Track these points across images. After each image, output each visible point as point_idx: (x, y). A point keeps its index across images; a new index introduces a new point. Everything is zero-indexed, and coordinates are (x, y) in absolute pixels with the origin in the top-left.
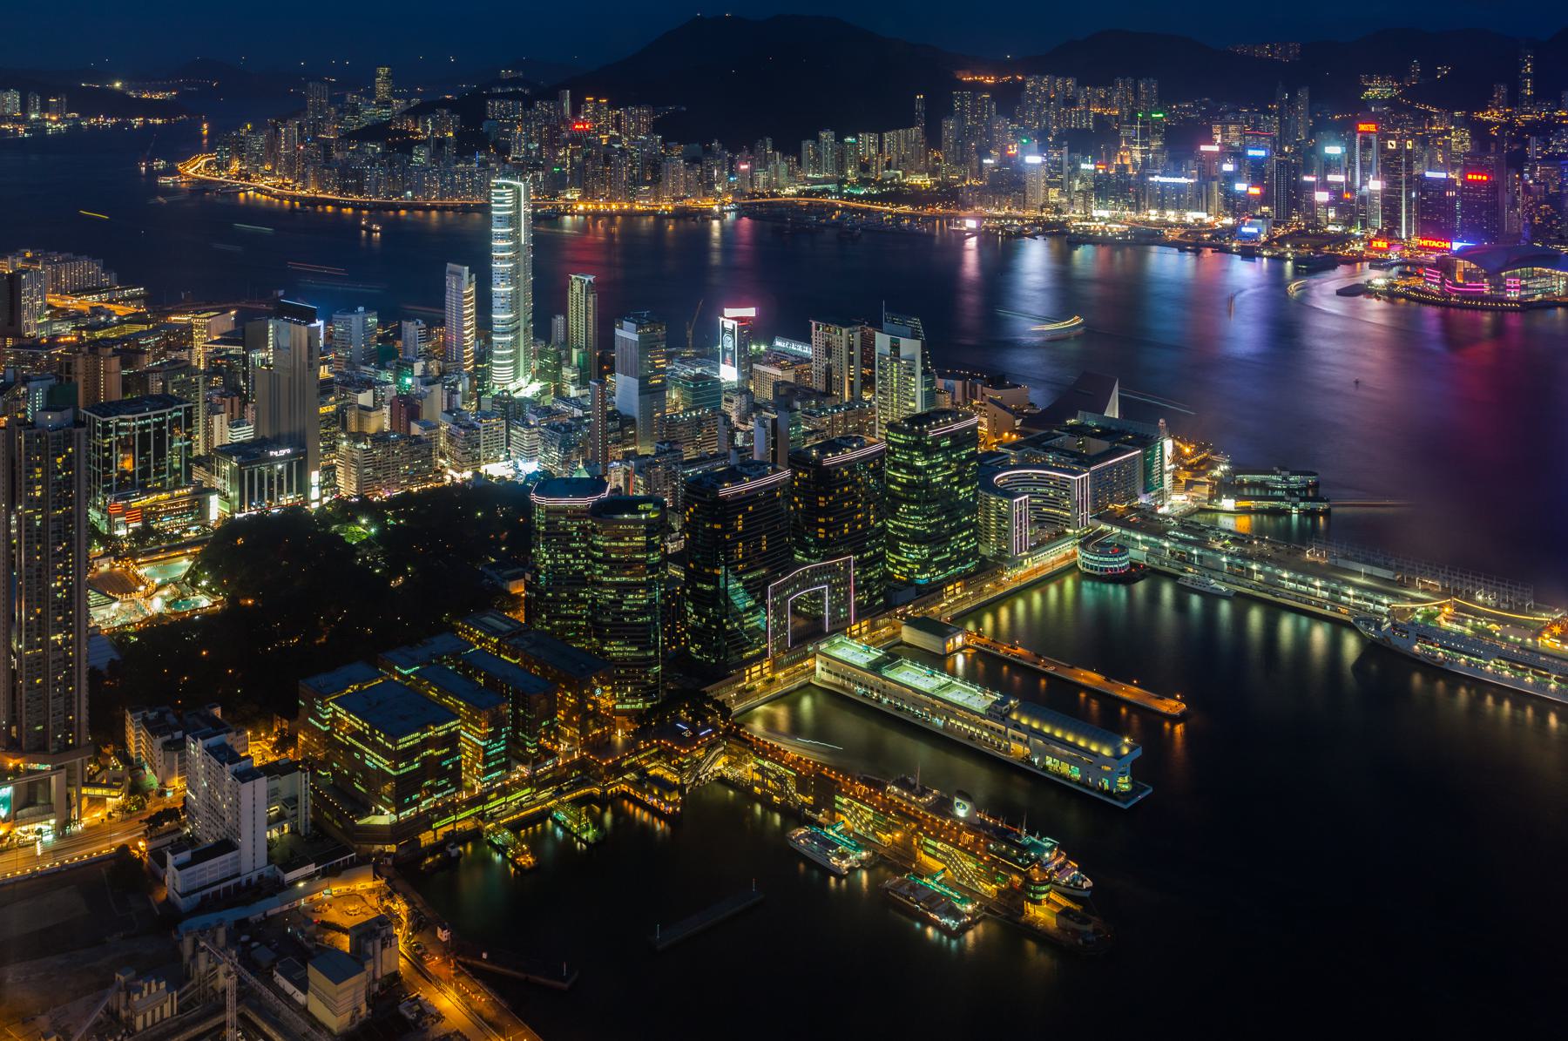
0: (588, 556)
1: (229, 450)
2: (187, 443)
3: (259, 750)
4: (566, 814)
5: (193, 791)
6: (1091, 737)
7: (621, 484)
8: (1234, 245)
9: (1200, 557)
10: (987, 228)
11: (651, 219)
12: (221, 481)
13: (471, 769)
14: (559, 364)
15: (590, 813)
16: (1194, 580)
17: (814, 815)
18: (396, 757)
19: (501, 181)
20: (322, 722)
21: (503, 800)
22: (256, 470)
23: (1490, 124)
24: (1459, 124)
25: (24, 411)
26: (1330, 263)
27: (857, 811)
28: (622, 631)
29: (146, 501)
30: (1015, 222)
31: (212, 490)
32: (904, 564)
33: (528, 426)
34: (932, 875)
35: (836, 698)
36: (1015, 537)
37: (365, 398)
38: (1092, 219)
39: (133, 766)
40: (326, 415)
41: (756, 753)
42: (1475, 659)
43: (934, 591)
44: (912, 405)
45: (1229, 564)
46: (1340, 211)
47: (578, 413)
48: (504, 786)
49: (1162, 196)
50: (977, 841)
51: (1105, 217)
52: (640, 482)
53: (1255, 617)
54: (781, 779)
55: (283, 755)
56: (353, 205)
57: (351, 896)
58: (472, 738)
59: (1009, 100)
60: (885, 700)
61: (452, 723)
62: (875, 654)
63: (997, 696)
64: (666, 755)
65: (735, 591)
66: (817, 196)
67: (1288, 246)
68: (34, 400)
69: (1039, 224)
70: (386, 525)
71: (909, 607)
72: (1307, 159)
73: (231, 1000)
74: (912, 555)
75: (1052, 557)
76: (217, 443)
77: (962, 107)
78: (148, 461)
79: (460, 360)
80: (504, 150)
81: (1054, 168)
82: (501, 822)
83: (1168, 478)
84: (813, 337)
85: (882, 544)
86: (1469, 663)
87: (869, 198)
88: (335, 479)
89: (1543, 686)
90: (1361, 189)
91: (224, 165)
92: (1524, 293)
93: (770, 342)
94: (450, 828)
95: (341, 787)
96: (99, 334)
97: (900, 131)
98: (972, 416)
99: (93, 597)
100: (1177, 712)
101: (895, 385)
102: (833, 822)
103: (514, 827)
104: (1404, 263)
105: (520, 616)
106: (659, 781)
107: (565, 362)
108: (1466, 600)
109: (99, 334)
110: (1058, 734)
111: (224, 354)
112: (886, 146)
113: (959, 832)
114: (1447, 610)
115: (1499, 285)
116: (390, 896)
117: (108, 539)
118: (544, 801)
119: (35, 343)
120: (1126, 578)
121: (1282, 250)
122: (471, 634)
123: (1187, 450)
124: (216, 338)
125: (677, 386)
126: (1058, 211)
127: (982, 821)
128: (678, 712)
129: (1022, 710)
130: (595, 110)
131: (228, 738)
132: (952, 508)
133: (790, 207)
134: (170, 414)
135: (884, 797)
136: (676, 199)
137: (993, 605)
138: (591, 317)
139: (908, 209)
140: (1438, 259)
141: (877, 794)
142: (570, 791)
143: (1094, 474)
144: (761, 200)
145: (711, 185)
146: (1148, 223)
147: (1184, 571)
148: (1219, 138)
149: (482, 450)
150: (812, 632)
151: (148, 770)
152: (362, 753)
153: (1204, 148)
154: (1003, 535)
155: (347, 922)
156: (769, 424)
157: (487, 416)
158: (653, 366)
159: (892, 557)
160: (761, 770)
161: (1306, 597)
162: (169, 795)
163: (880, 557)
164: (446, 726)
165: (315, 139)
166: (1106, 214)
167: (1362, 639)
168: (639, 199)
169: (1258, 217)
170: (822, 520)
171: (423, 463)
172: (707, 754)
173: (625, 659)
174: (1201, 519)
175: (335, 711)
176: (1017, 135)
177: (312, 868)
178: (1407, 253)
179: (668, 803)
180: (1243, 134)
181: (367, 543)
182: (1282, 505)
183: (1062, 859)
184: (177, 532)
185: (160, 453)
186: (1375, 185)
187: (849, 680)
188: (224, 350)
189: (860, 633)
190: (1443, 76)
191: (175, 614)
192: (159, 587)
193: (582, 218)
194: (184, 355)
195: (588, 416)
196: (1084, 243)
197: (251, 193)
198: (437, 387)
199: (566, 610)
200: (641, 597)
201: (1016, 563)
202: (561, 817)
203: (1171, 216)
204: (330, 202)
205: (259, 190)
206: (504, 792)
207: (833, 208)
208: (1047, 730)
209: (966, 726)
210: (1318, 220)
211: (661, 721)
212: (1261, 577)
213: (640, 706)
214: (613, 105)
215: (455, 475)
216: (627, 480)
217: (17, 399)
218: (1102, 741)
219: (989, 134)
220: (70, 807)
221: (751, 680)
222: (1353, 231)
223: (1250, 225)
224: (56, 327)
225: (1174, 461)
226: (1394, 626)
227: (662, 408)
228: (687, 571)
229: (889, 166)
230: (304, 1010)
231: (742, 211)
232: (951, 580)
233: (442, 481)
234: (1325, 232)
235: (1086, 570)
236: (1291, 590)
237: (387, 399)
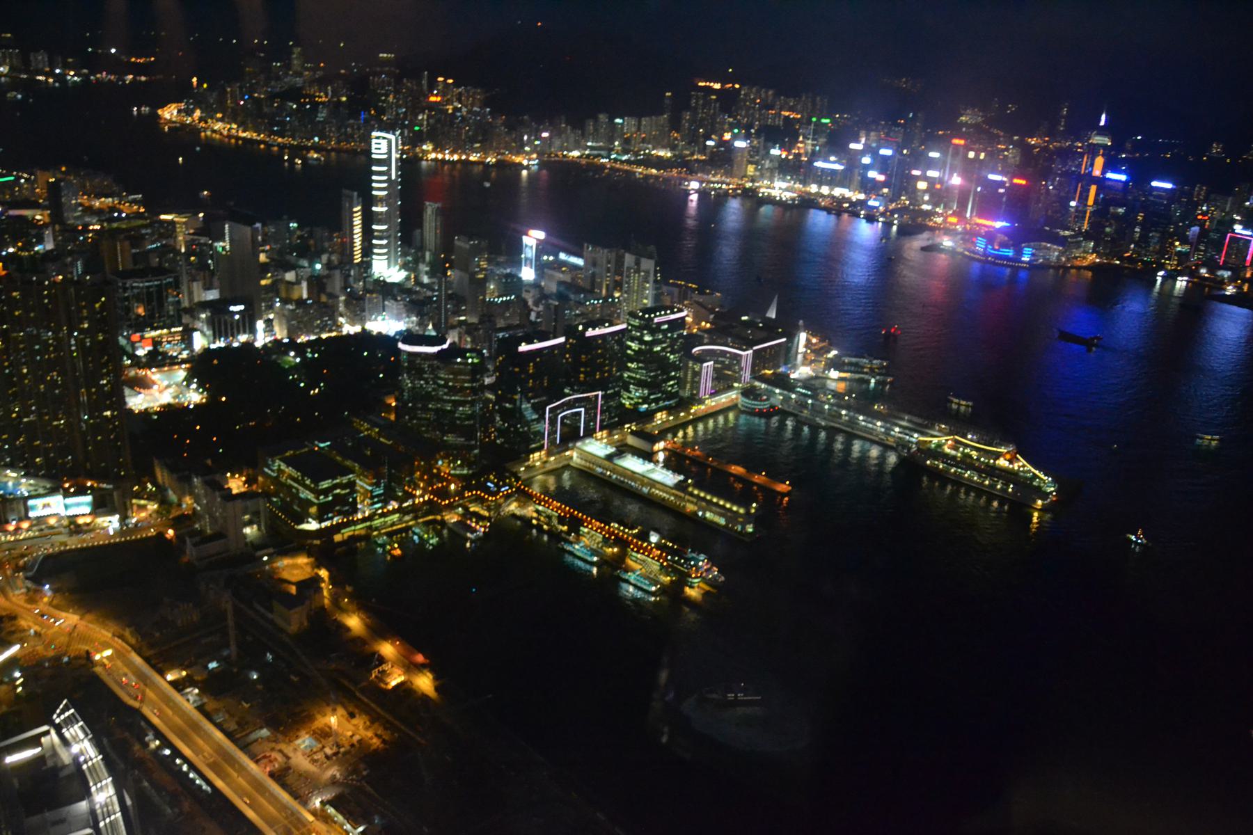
0: (435, 383)
1: (205, 305)
2: (177, 299)
3: (236, 484)
4: (420, 528)
5: (198, 504)
6: (734, 502)
7: (456, 340)
8: (863, 212)
9: (812, 404)
10: (704, 188)
11: (481, 167)
12: (201, 324)
13: (362, 502)
14: (417, 261)
15: (434, 529)
16: (806, 418)
17: (567, 537)
18: (318, 493)
19: (379, 134)
20: (273, 471)
21: (382, 520)
22: (222, 320)
23: (1034, 147)
24: (1015, 144)
25: (72, 273)
26: (922, 228)
27: (592, 536)
28: (454, 429)
29: (154, 334)
30: (724, 186)
31: (196, 330)
32: (632, 399)
33: (396, 300)
34: (633, 571)
35: (584, 474)
36: (702, 386)
37: (290, 276)
38: (774, 188)
39: (161, 490)
40: (266, 286)
41: (535, 502)
42: (959, 470)
43: (650, 415)
44: (645, 301)
45: (829, 409)
46: (932, 196)
47: (429, 293)
48: (383, 512)
49: (821, 176)
50: (661, 554)
51: (781, 189)
52: (469, 339)
53: (840, 438)
54: (549, 517)
55: (250, 488)
56: (278, 145)
57: (295, 566)
58: (363, 484)
59: (728, 101)
60: (614, 477)
61: (351, 476)
62: (611, 450)
63: (681, 478)
64: (479, 500)
65: (527, 409)
66: (593, 159)
67: (896, 216)
68: (77, 267)
69: (739, 189)
70: (307, 357)
71: (634, 424)
72: (919, 159)
73: (230, 616)
74: (636, 393)
75: (724, 399)
76: (196, 300)
77: (696, 103)
78: (153, 309)
79: (352, 255)
80: (381, 111)
81: (753, 151)
82: (383, 531)
83: (800, 357)
84: (585, 253)
85: (619, 386)
86: (956, 472)
87: (628, 162)
88: (273, 326)
89: (993, 486)
90: (947, 182)
91: (189, 113)
92: (1033, 258)
93: (556, 255)
94: (351, 533)
95: (285, 507)
96: (115, 225)
97: (653, 117)
98: (680, 310)
99: (127, 391)
100: (785, 491)
101: (636, 288)
102: (578, 541)
103: (390, 535)
104: (965, 232)
105: (392, 417)
106: (475, 514)
107: (421, 260)
108: (962, 437)
109: (115, 225)
110: (715, 500)
111: (197, 242)
112: (642, 127)
113: (652, 548)
114: (950, 442)
115: (1019, 252)
116: (319, 567)
117: (133, 357)
118: (407, 522)
119: (74, 229)
120: (767, 414)
121: (891, 218)
122: (362, 425)
123: (814, 340)
124: (192, 231)
125: (494, 280)
126: (753, 181)
127: (665, 544)
128: (489, 477)
129: (695, 486)
130: (444, 87)
131: (217, 477)
132: (663, 365)
133: (574, 164)
134: (165, 279)
135: (609, 529)
136: (498, 154)
137: (684, 426)
138: (438, 231)
139: (654, 171)
140: (986, 232)
141: (604, 527)
142: (423, 517)
143: (755, 351)
144: (556, 159)
145: (523, 145)
146: (810, 194)
147: (802, 412)
148: (863, 140)
149: (366, 313)
150: (571, 436)
151: (170, 492)
152: (298, 490)
153: (853, 146)
154: (696, 385)
155: (294, 579)
156: (552, 307)
157: (371, 292)
158: (479, 266)
159: (625, 395)
160: (537, 511)
161: (870, 431)
162: (184, 506)
163: (618, 394)
164: (348, 477)
165: (251, 97)
166: (784, 185)
167: (899, 457)
168: (473, 152)
169: (878, 195)
170: (582, 369)
171: (329, 320)
172: (505, 501)
173: (456, 445)
174: (817, 383)
175: (279, 466)
176: (730, 130)
177: (271, 550)
178: (968, 226)
179: (481, 526)
180: (879, 140)
181: (295, 368)
182: (866, 377)
183: (709, 566)
184: (175, 354)
185: (161, 304)
186: (956, 180)
187: (593, 464)
188: (196, 240)
189: (602, 439)
190: (1012, 111)
191: (178, 403)
192: (168, 387)
193: (433, 163)
194: (171, 242)
195: (435, 296)
196: (767, 203)
197: (209, 133)
198: (337, 273)
199: (420, 414)
200: (466, 409)
201: (701, 402)
202: (417, 530)
203: (825, 190)
204: (261, 142)
205: (214, 131)
206: (383, 515)
207: (603, 166)
208: (708, 497)
209: (661, 493)
210: (917, 200)
211: (478, 482)
212: (847, 418)
213: (465, 472)
214: (456, 85)
215: (349, 329)
216: (460, 338)
217: (66, 265)
218: (740, 505)
219: (713, 124)
220: (126, 510)
221: (534, 461)
222: (937, 210)
223: (875, 200)
224: (87, 219)
225: (806, 346)
226: (919, 450)
227: (484, 294)
228: (496, 395)
229: (643, 141)
230: (272, 622)
231: (542, 165)
232: (660, 410)
233: (341, 331)
234: (922, 210)
235: (743, 409)
236: (863, 426)
237: (305, 277)
